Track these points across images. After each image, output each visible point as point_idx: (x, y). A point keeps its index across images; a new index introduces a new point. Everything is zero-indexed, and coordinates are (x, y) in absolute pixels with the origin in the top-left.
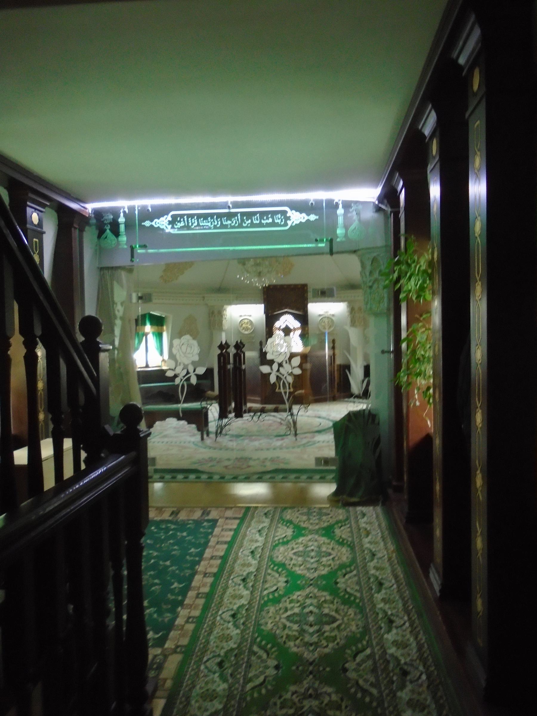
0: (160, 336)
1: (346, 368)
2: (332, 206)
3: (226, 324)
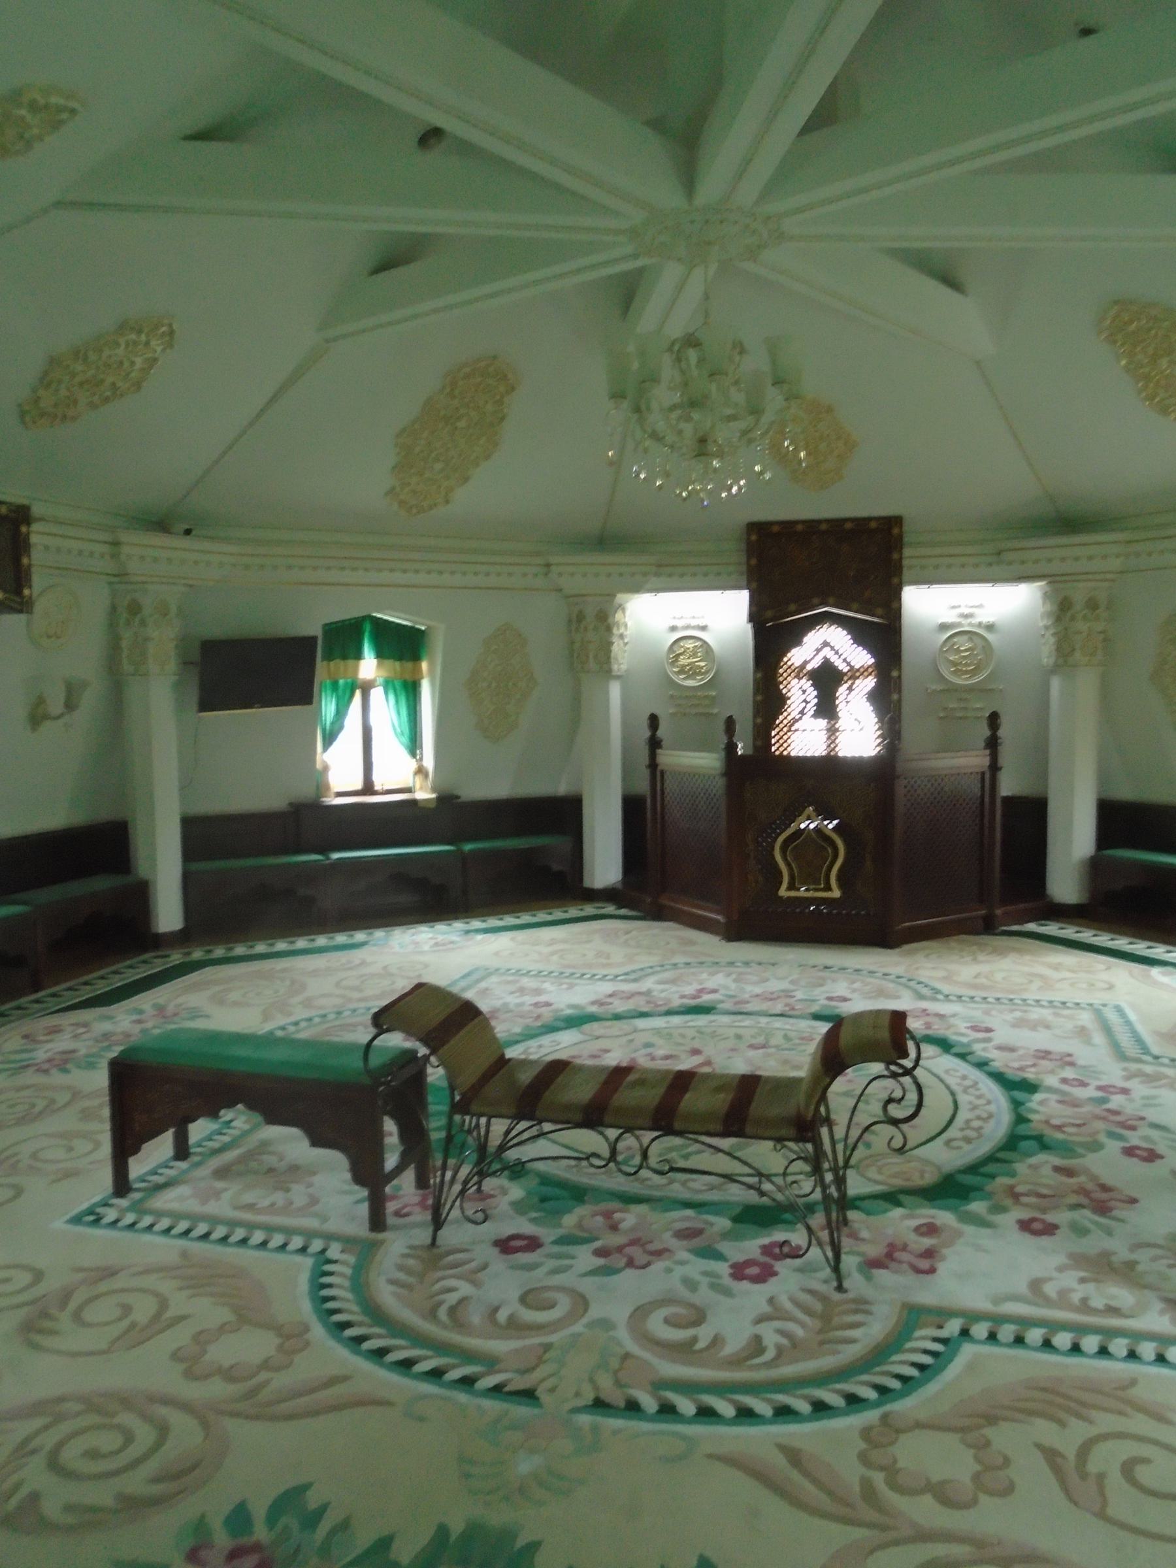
0: (411, 690)
3: (623, 657)
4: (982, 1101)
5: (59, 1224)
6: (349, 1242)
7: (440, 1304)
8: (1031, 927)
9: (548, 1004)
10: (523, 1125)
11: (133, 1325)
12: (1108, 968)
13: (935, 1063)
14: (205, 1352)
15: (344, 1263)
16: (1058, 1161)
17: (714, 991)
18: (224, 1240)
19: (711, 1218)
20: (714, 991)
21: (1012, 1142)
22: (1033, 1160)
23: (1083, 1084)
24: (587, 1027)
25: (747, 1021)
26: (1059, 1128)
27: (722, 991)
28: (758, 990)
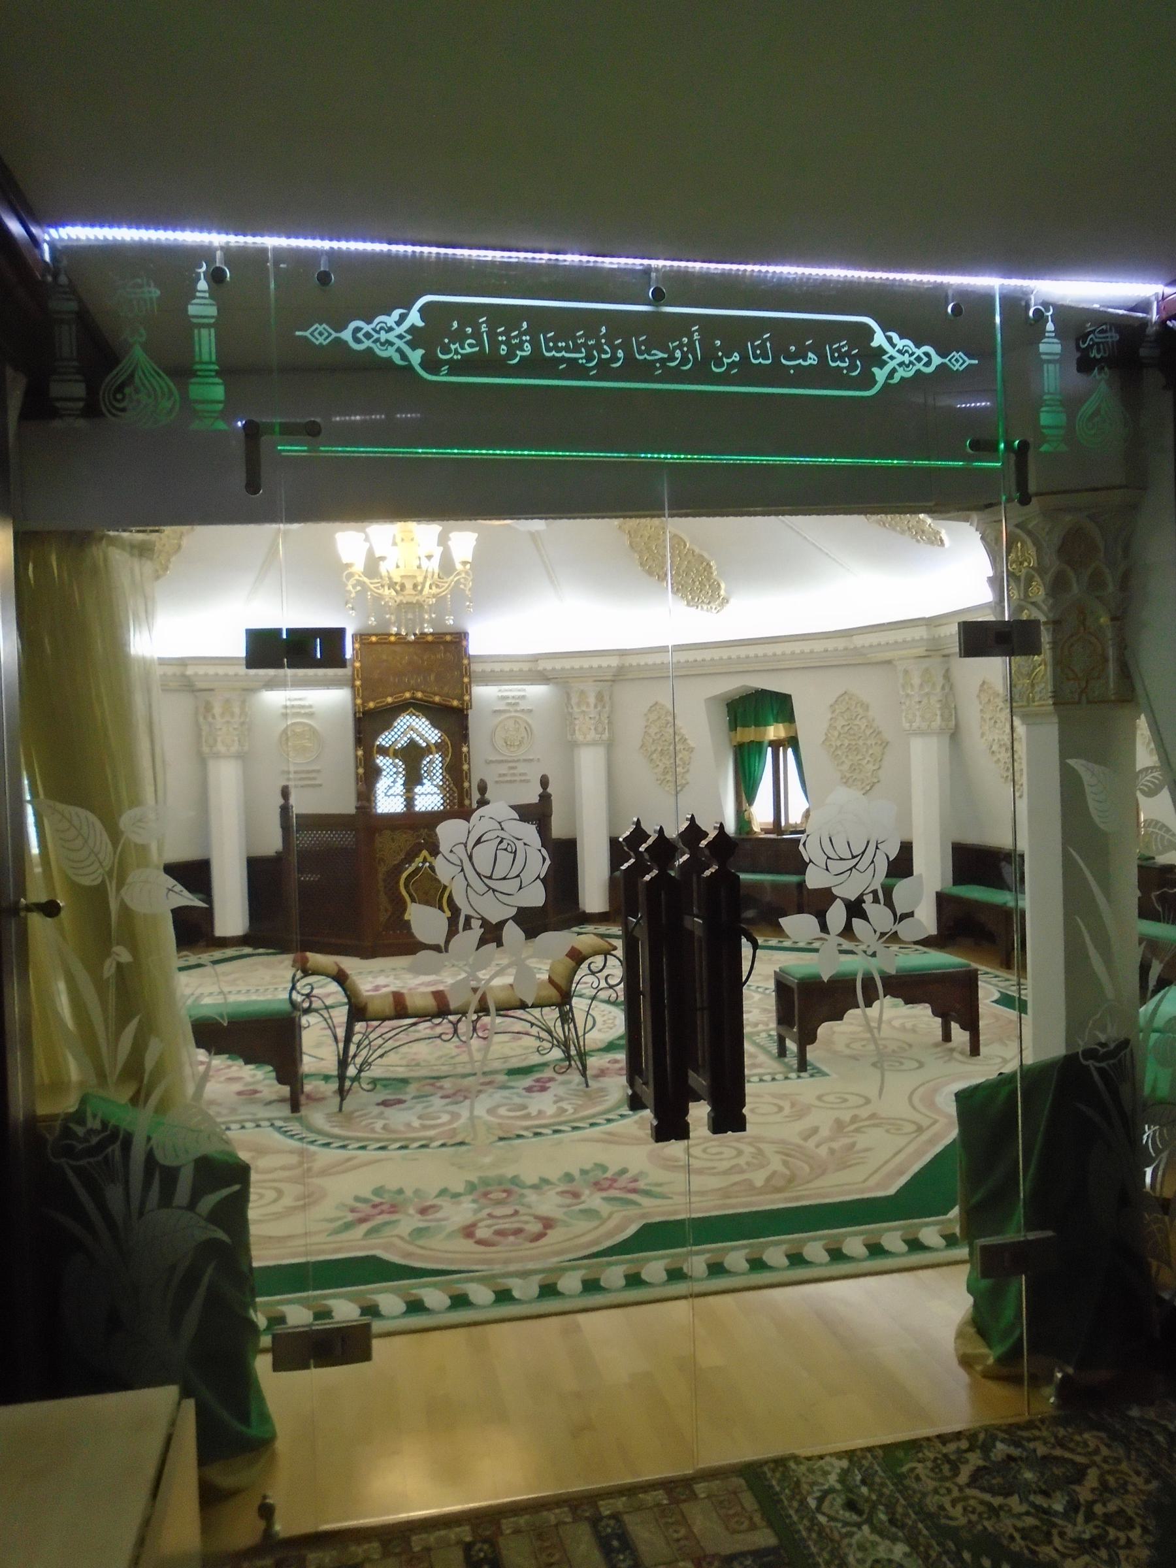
2: (1025, 322)
17: (385, 986)
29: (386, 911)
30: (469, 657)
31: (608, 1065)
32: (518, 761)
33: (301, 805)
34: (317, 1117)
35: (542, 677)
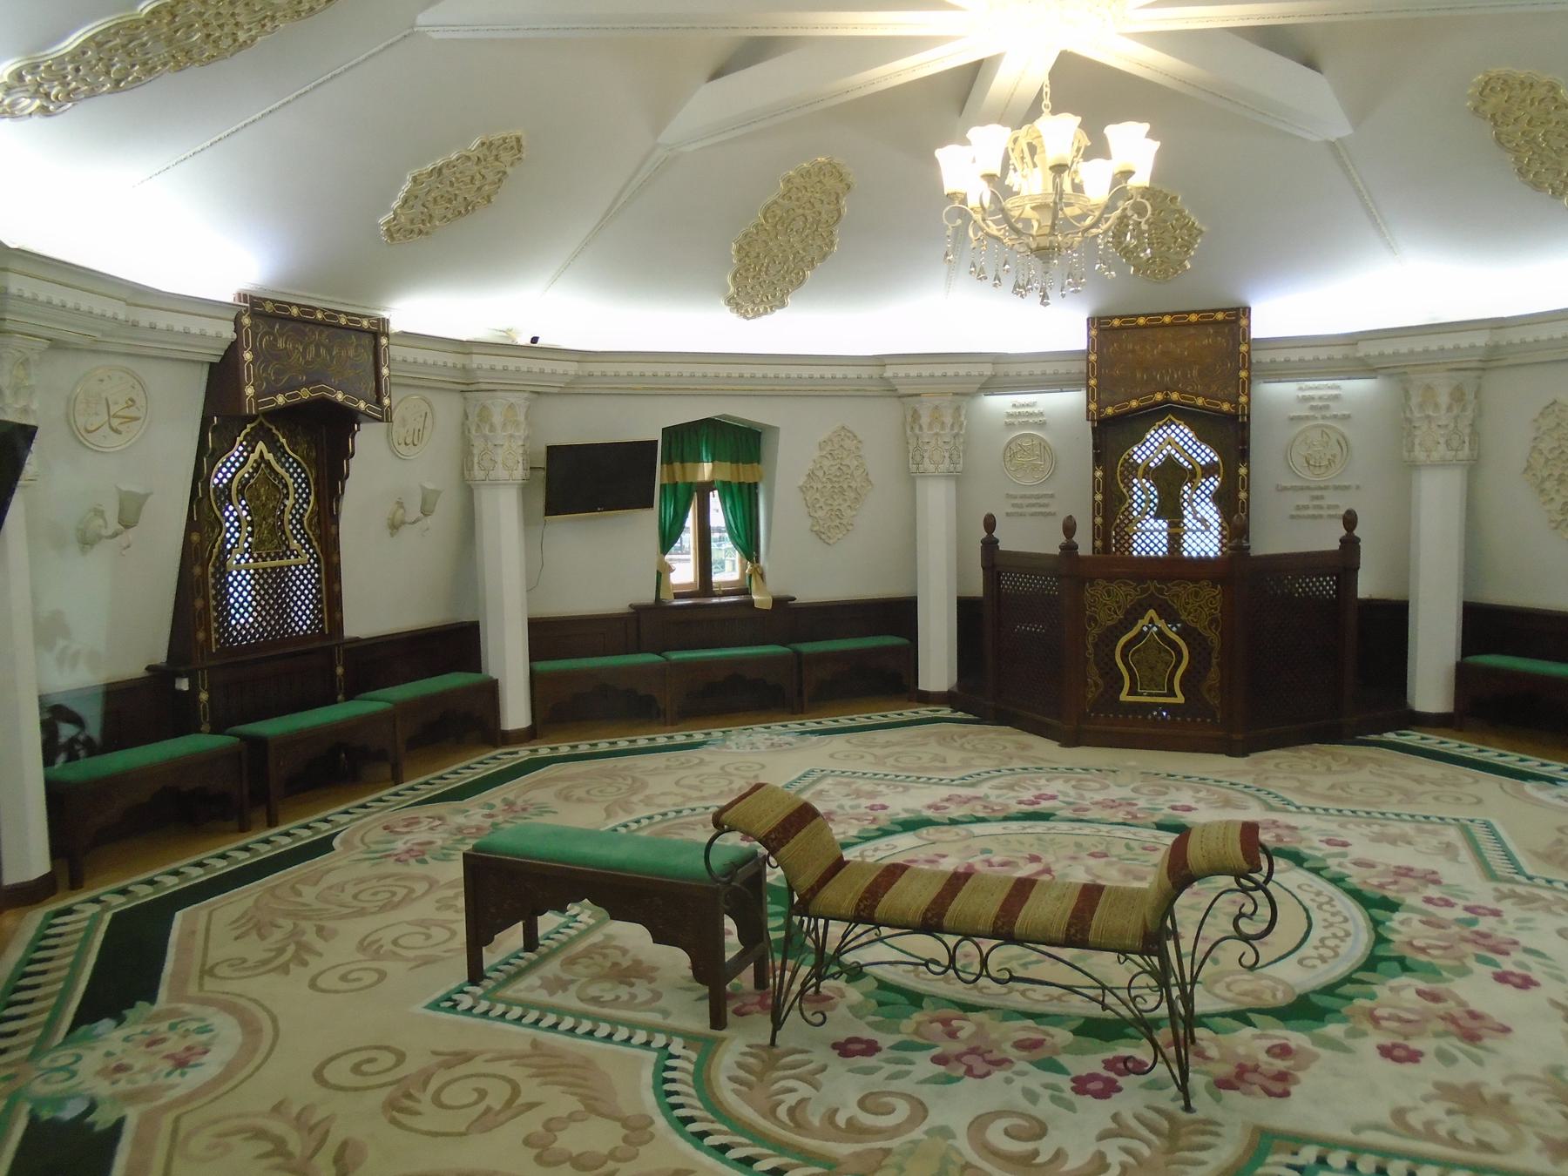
1: (1392, 619)
4: (1339, 919)
5: (419, 1008)
6: (690, 1039)
7: (779, 1103)
8: (1390, 736)
9: (884, 807)
10: (859, 929)
11: (488, 1110)
12: (1477, 781)
13: (1287, 877)
14: (555, 1139)
15: (687, 1059)
16: (1422, 986)
17: (1053, 797)
18: (572, 1031)
19: (1051, 1030)
20: (1053, 797)
21: (1371, 963)
22: (1395, 982)
23: (1448, 904)
24: (924, 831)
25: (1087, 829)
26: (1423, 950)
27: (1061, 798)
28: (1098, 797)
29: (1096, 685)
30: (1249, 342)
31: (1263, 1058)
32: (1326, 488)
33: (1010, 540)
34: (738, 1045)
35: (1365, 368)
